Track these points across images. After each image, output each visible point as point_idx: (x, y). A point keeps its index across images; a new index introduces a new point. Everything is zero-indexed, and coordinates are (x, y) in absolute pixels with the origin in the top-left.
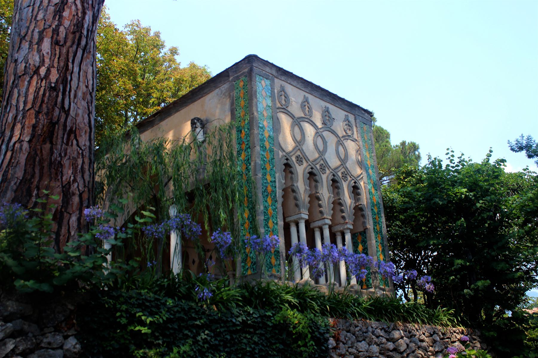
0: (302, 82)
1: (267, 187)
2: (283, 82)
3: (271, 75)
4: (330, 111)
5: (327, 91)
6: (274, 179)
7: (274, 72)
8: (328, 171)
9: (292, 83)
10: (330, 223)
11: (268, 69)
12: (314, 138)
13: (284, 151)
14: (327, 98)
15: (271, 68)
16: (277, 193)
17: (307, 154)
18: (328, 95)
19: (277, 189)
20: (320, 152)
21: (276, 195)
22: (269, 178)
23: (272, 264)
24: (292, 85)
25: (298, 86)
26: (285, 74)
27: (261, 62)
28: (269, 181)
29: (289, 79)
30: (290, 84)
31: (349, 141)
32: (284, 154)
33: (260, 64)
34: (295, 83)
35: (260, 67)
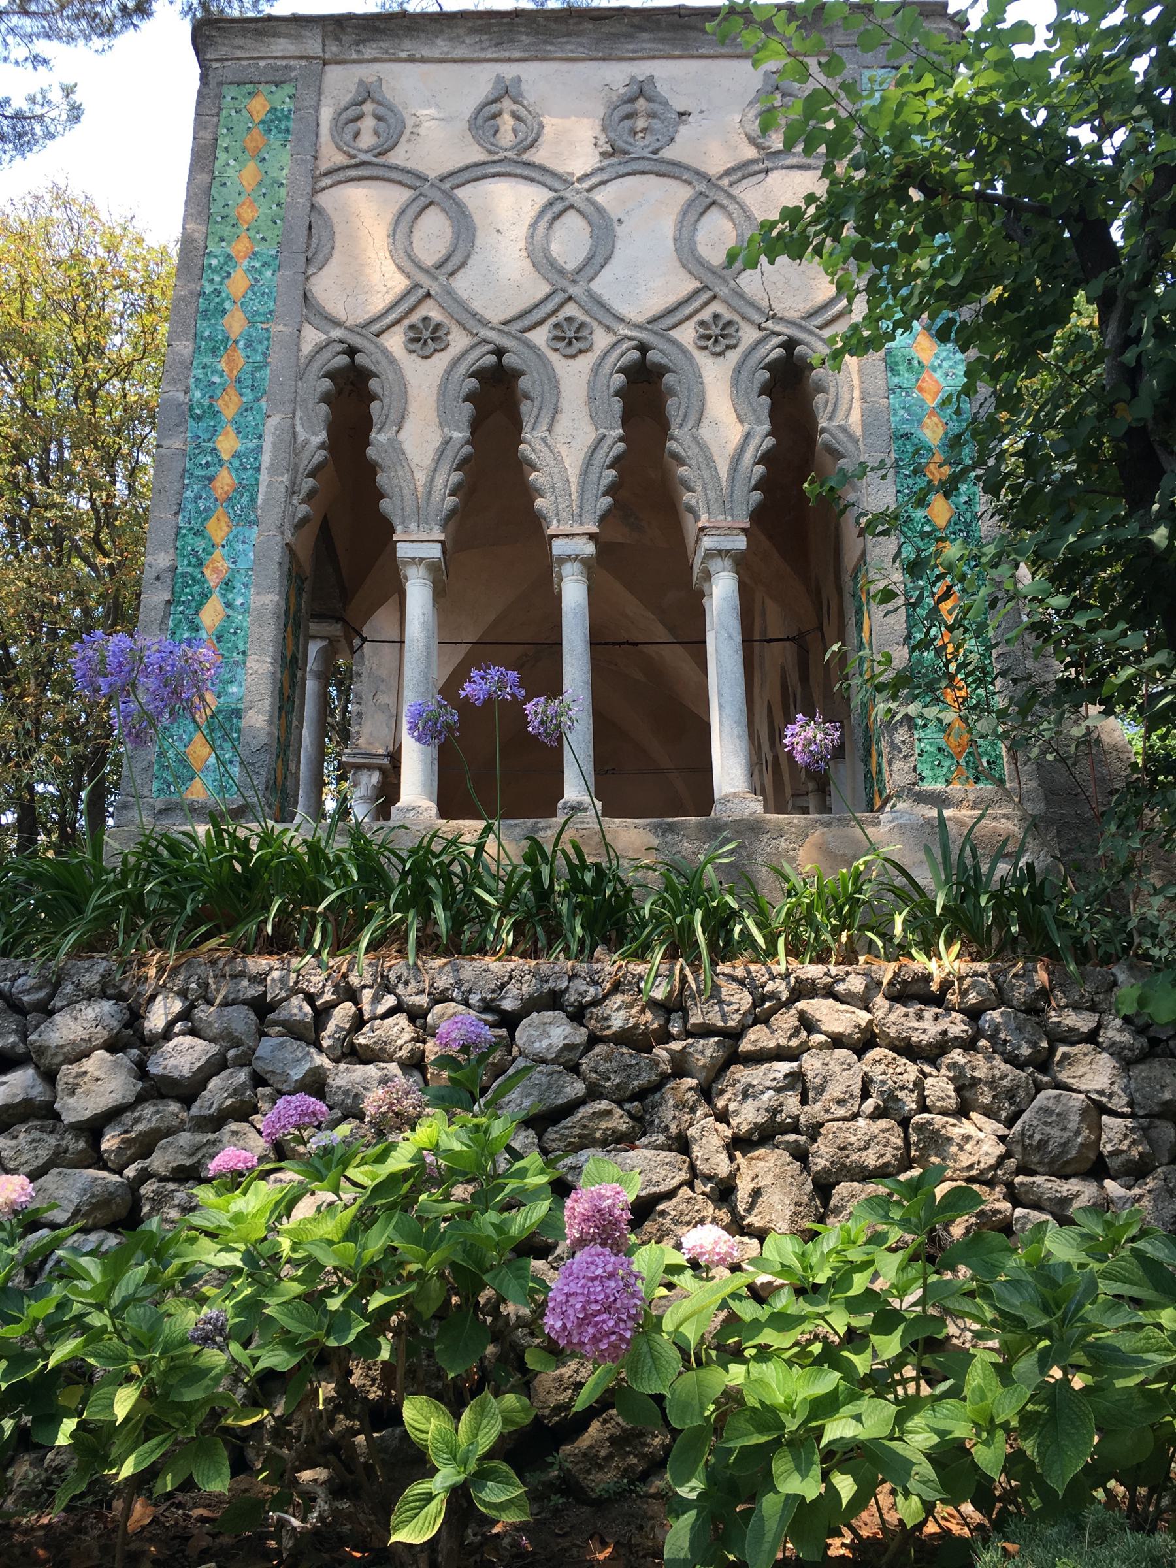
0: (473, 31)
1: (211, 479)
2: (377, 66)
3: (303, 63)
4: (662, 89)
5: (622, 11)
6: (251, 445)
7: (313, 45)
8: (601, 340)
9: (426, 52)
10: (589, 549)
11: (281, 46)
12: (534, 225)
13: (337, 324)
14: (645, 40)
15: (298, 37)
16: (262, 489)
17: (477, 306)
18: (641, 29)
19: (264, 476)
20: (561, 272)
21: (253, 500)
22: (227, 444)
23: (188, 767)
24: (423, 60)
25: (460, 52)
26: (383, 32)
27: (244, 33)
28: (225, 457)
29: (407, 44)
30: (411, 60)
31: (774, 176)
32: (336, 333)
33: (239, 41)
34: (441, 47)
35: (239, 54)
